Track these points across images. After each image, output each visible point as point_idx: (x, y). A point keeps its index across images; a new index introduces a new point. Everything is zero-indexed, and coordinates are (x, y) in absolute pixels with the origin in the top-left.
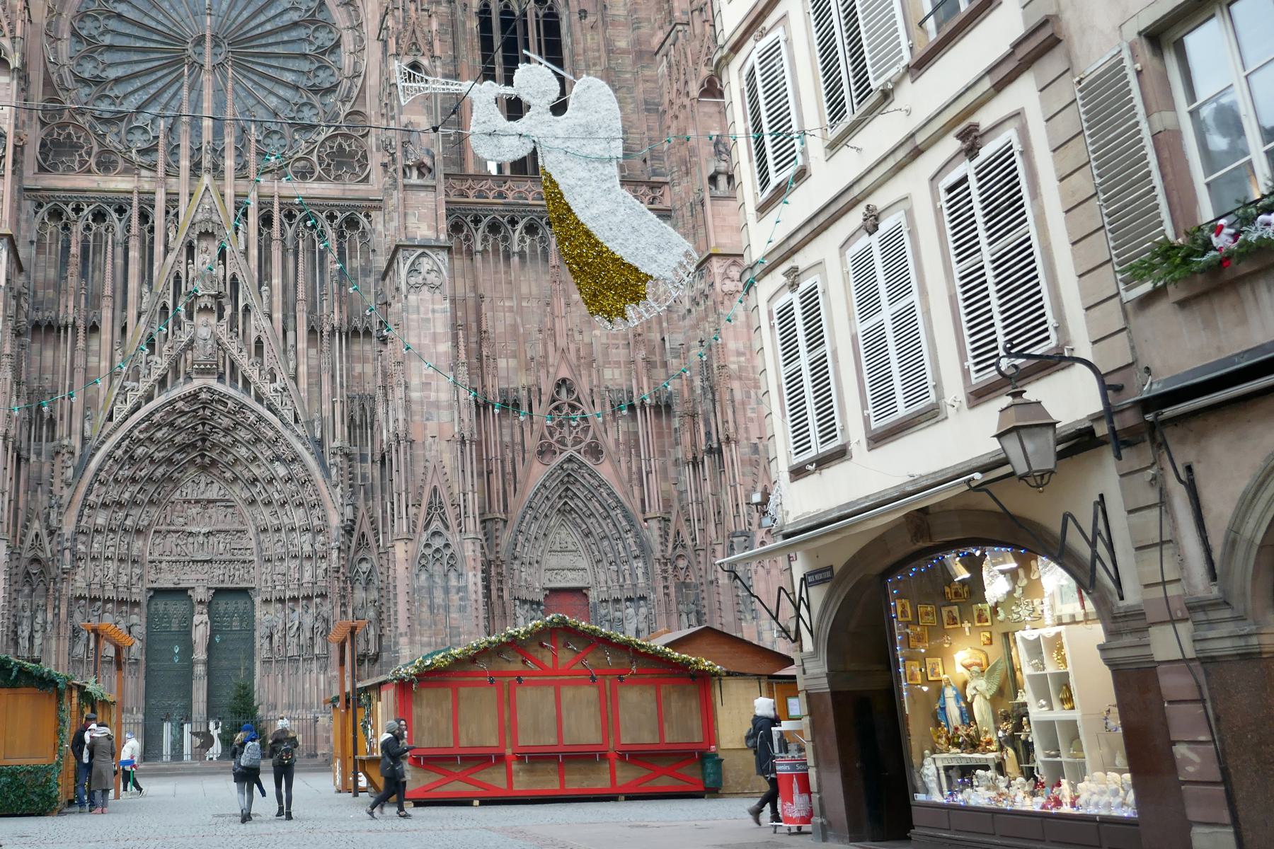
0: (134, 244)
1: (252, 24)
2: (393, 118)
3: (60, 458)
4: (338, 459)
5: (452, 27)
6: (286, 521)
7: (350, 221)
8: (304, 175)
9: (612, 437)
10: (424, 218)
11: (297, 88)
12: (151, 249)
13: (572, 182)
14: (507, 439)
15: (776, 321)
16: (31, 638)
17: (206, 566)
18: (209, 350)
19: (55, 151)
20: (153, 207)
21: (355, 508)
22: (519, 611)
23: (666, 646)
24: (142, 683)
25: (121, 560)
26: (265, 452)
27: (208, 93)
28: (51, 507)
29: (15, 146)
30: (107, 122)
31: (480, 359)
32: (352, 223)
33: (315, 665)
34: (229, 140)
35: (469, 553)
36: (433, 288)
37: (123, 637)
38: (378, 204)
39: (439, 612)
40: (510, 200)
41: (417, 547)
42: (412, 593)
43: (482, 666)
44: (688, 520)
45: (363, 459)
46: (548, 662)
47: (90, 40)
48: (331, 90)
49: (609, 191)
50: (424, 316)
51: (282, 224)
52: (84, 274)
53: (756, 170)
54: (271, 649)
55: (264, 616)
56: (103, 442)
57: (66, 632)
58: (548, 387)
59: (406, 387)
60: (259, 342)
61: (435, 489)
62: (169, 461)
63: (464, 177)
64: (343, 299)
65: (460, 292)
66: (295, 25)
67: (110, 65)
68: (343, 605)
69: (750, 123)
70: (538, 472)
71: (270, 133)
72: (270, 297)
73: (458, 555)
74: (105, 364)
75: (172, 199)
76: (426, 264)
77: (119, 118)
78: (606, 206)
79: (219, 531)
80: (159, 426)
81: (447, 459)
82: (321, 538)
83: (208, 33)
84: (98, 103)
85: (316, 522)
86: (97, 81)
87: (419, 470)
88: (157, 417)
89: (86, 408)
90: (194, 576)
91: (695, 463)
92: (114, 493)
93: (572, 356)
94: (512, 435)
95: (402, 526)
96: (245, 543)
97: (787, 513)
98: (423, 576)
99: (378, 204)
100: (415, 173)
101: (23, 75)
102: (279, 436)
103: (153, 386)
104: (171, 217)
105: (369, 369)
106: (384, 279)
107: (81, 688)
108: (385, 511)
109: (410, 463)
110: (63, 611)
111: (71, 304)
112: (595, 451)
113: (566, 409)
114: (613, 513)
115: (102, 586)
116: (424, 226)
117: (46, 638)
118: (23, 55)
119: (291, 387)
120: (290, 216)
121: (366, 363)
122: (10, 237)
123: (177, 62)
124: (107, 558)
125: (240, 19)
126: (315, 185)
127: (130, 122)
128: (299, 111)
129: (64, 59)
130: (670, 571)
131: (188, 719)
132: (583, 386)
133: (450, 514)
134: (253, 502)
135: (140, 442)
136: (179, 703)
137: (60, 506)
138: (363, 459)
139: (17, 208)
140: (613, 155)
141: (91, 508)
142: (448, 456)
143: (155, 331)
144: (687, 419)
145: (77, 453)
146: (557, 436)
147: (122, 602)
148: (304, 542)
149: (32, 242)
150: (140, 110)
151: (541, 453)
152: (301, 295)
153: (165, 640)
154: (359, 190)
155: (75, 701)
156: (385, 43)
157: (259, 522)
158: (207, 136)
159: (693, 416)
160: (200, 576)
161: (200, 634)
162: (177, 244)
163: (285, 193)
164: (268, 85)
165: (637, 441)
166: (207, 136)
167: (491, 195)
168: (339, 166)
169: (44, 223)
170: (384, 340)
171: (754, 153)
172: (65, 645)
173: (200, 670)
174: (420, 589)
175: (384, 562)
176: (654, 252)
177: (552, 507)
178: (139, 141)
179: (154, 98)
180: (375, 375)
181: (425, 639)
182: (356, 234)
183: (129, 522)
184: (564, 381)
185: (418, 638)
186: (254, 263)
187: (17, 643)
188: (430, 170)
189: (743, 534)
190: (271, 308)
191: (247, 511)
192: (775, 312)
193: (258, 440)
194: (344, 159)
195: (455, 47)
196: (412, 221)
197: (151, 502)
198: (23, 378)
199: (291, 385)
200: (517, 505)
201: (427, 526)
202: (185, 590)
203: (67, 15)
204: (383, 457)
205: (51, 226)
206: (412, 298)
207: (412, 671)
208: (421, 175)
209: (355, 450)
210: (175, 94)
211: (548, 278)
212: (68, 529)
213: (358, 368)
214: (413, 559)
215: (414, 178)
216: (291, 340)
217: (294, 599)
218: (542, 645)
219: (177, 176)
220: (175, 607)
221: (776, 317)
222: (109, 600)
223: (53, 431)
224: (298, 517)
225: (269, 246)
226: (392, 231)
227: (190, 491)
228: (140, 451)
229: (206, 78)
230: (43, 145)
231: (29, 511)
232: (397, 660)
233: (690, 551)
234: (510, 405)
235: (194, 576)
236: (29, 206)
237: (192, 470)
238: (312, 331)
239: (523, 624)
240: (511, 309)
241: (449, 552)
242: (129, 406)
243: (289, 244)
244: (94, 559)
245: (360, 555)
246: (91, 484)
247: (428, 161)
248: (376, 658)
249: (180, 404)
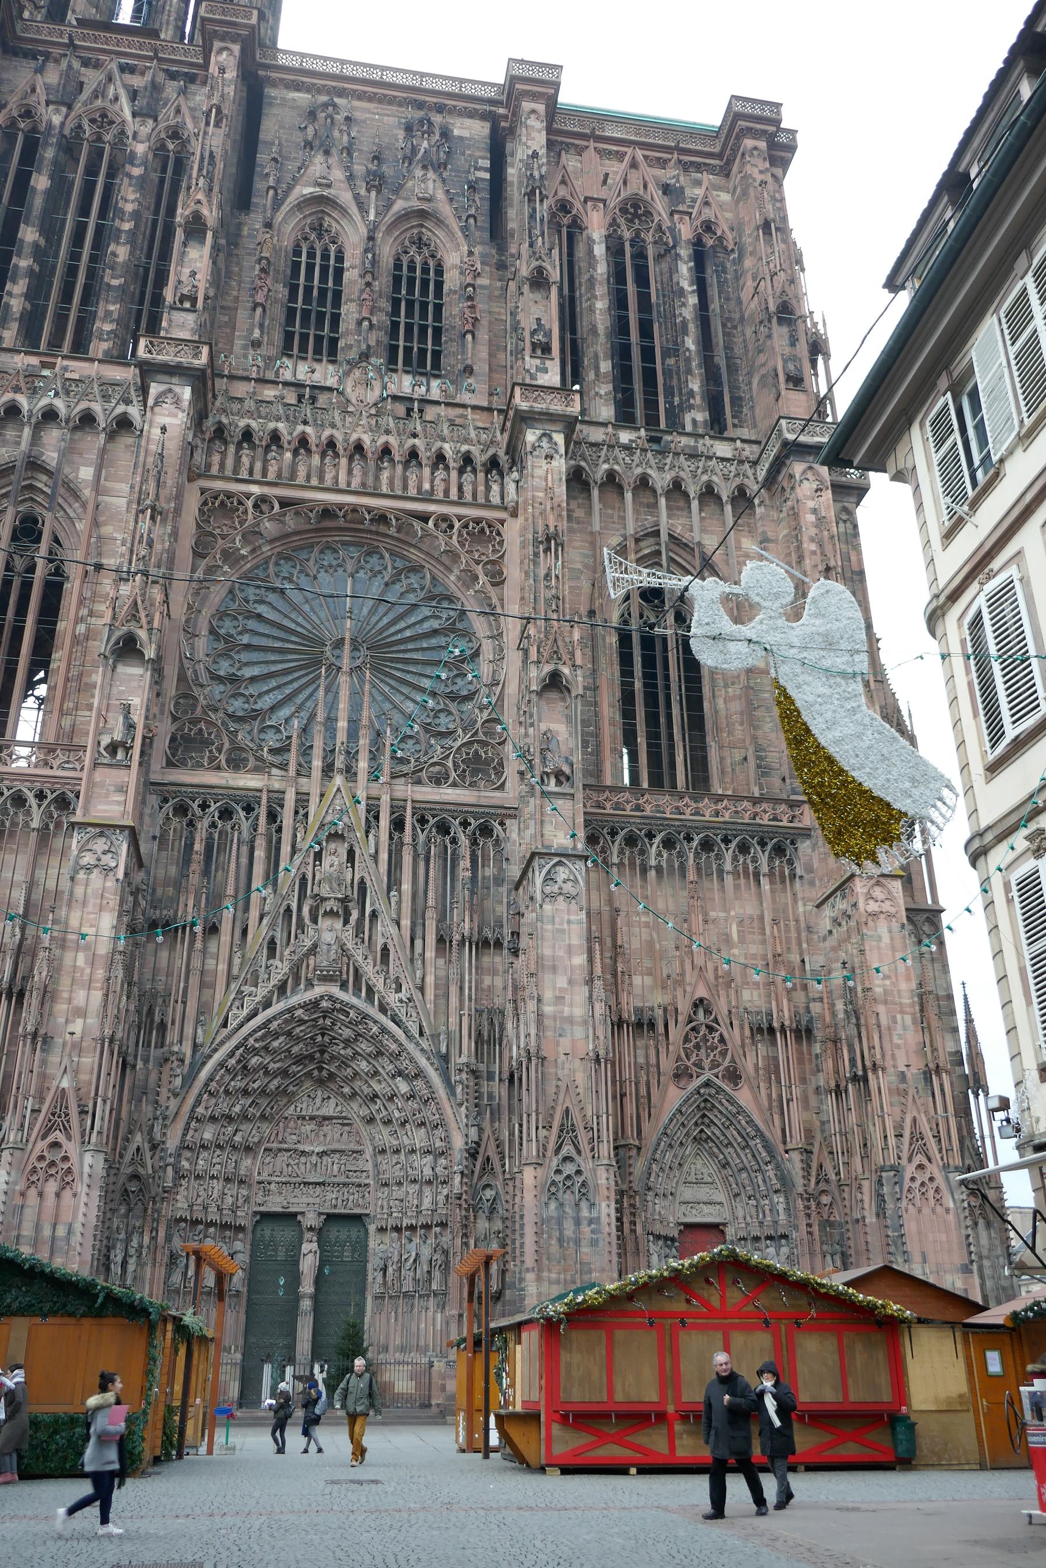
0: (260, 843)
1: (392, 630)
2: (532, 725)
3: (169, 1065)
4: (464, 1076)
5: (592, 642)
6: (406, 1141)
7: (485, 828)
8: (438, 780)
9: (752, 1060)
10: (561, 827)
11: (433, 694)
12: (278, 849)
13: (811, 698)
14: (641, 1060)
15: (1015, 893)
16: (124, 1264)
17: (318, 1189)
18: (333, 956)
19: (185, 746)
20: (282, 806)
21: (481, 1130)
22: (653, 1248)
23: (848, 1284)
24: (243, 1317)
25: (227, 1180)
26: (386, 1066)
27: (344, 694)
28: (156, 1118)
29: (144, 738)
30: (240, 720)
31: (615, 975)
32: (486, 830)
33: (432, 1302)
34: (364, 742)
35: (602, 1181)
36: (569, 898)
37: (227, 1265)
38: (513, 813)
39: (566, 1247)
40: (648, 813)
41: (546, 1173)
42: (541, 1223)
43: (639, 1305)
45: (490, 1077)
46: (715, 1302)
47: (228, 639)
48: (469, 697)
49: (854, 711)
50: (559, 927)
51: (414, 828)
52: (206, 873)
53: (984, 725)
54: (385, 1283)
55: (378, 1246)
56: (215, 1050)
57: (163, 1258)
58: (684, 1007)
59: (539, 1001)
60: (385, 950)
61: (567, 1110)
62: (284, 1073)
63: (601, 788)
64: (476, 908)
65: (595, 905)
66: (435, 632)
67: (247, 664)
68: (465, 1235)
69: (974, 675)
70: (673, 1097)
71: (406, 738)
72: (399, 903)
73: (590, 1183)
74: (222, 967)
75: (302, 800)
76: (562, 873)
77: (254, 715)
78: (851, 729)
79: (334, 1151)
80: (276, 1035)
81: (581, 1078)
82: (442, 1161)
83: (347, 636)
84: (232, 701)
85: (438, 1144)
86: (233, 679)
87: (551, 1090)
88: (274, 1025)
89: (200, 1012)
90: (305, 1200)
91: (839, 1091)
92: (223, 1106)
93: (710, 975)
94: (647, 1056)
95: (531, 1150)
96: (360, 1164)
97: (1038, 1120)
98: (553, 1206)
99: (513, 813)
100: (553, 781)
101: (157, 667)
102: (402, 1048)
103: (271, 992)
104: (300, 817)
105: (499, 982)
106: (517, 889)
107: (177, 1320)
108: (512, 1134)
109: (542, 1081)
110: (162, 1234)
111: (191, 903)
112: (734, 1076)
113: (703, 1030)
114: (752, 1143)
115: (205, 1208)
116: (561, 834)
117: (140, 1264)
118: (159, 647)
119: (417, 997)
120: (423, 821)
121: (497, 975)
122: (132, 829)
123: (316, 663)
124: (213, 1177)
125: (380, 625)
126: (450, 791)
127: (263, 720)
128: (436, 717)
129: (200, 655)
131: (291, 1360)
132: (721, 1007)
133: (583, 1137)
134: (371, 1120)
135: (255, 1052)
136: (282, 1342)
137: (165, 1118)
138: (490, 1077)
139: (141, 802)
140: (857, 670)
141: (198, 1121)
142: (581, 1075)
143: (278, 935)
144: (830, 1044)
145: (187, 1061)
146: (694, 1058)
147: (226, 1226)
148: (424, 1166)
149: (154, 838)
150: (273, 709)
151: (677, 1076)
152: (431, 902)
153: (271, 1267)
154: (495, 797)
155: (169, 1335)
156: (526, 652)
157: (377, 1142)
158: (341, 736)
159: (836, 1041)
160: (311, 1200)
161: (308, 1264)
162: (305, 843)
163: (418, 797)
164: (405, 690)
165: (777, 1067)
166: (341, 736)
167: (628, 807)
168: (475, 772)
169: (168, 819)
170: (515, 952)
171: (980, 706)
172: (161, 1272)
173: (306, 1304)
174: (550, 1219)
175: (510, 1189)
176: (908, 785)
177: (687, 1134)
178: (272, 740)
179: (289, 698)
180: (505, 988)
181: (554, 1276)
182: (490, 843)
183: (238, 1138)
184: (701, 1000)
185: (545, 1274)
186: (383, 867)
187: (108, 1269)
188: (568, 778)
189: (893, 1168)
190: (399, 914)
191: (364, 1130)
192: (1013, 883)
193: (379, 1053)
194: (480, 766)
195: (594, 660)
196: (548, 829)
197: (263, 1117)
198: (136, 978)
199: (417, 995)
200: (651, 1131)
201: (557, 1151)
202: (294, 1215)
203: (206, 613)
204: (512, 1076)
205: (175, 822)
206: (547, 907)
207: (561, 1308)
208: (559, 783)
209: (482, 1067)
210: (311, 695)
211: (685, 893)
212: (172, 1143)
213: (487, 981)
214: (543, 1186)
215: (552, 786)
216: (418, 949)
217: (412, 1228)
218: (708, 1282)
219: (309, 776)
220: (283, 1234)
221: (1015, 888)
222: (212, 1224)
223: (164, 1037)
224: (419, 1138)
225: (399, 852)
226: (527, 840)
227: (304, 1107)
228: (255, 1061)
229: (343, 679)
230: (173, 739)
231: (132, 1122)
232: (522, 1299)
233: (833, 1187)
234: (644, 1025)
235: (305, 1200)
236: (154, 800)
237: (308, 1084)
238: (440, 940)
239: (659, 1263)
240: (647, 925)
241: (581, 1179)
242: (245, 1012)
243: (420, 849)
244: (198, 1177)
245: (485, 1180)
246: (200, 1095)
247: (566, 769)
248: (498, 1296)
249: (299, 1012)
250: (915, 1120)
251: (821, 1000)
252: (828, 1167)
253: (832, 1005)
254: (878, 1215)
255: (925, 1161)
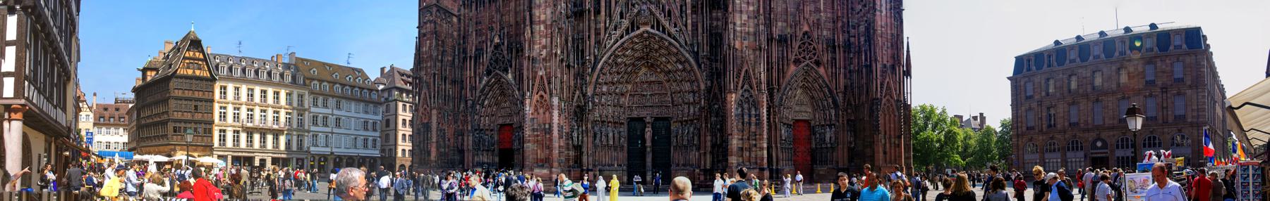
161: (648, 135)
220: (638, 126)
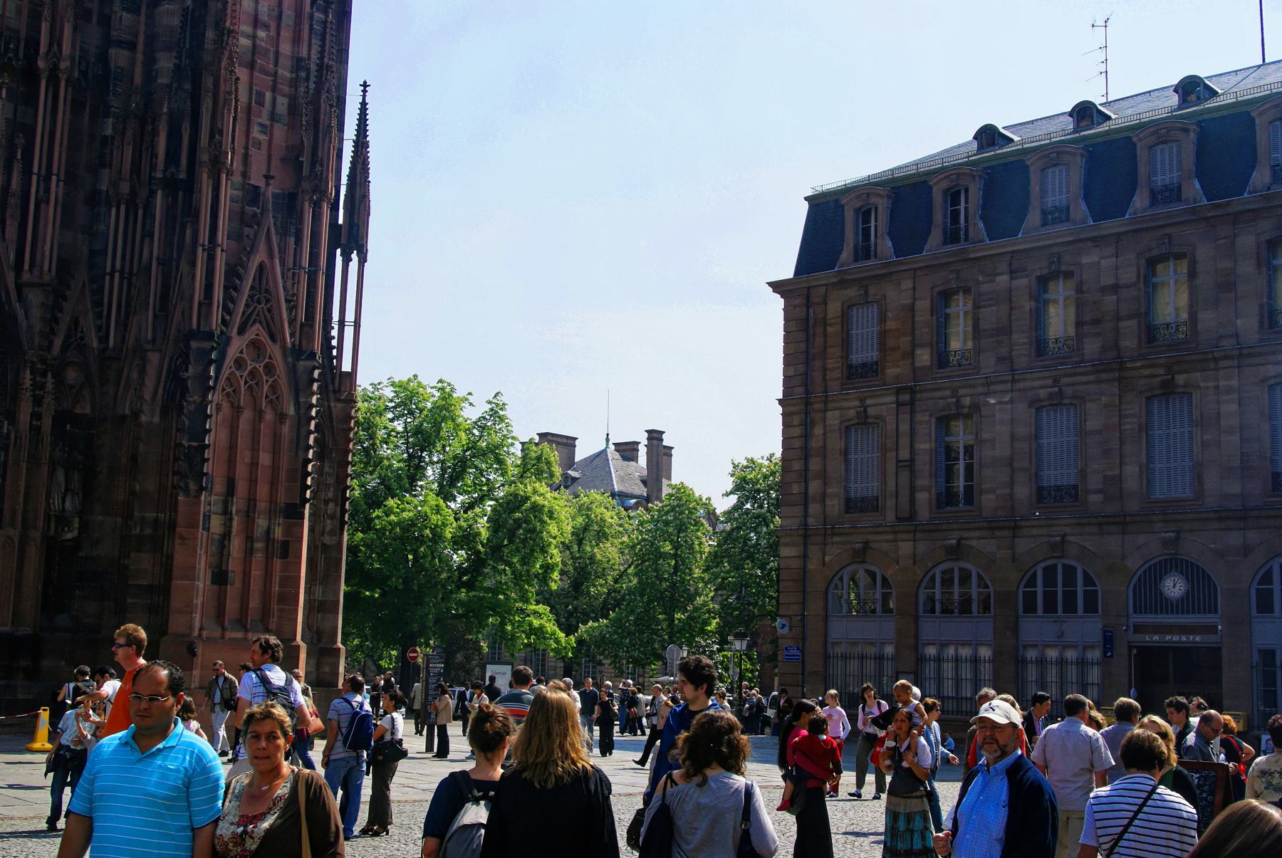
44: (98, 304)
130: (50, 386)
250: (261, 268)
251: (132, 46)
252: (89, 324)
253: (150, 60)
254: (165, 412)
255: (264, 337)
